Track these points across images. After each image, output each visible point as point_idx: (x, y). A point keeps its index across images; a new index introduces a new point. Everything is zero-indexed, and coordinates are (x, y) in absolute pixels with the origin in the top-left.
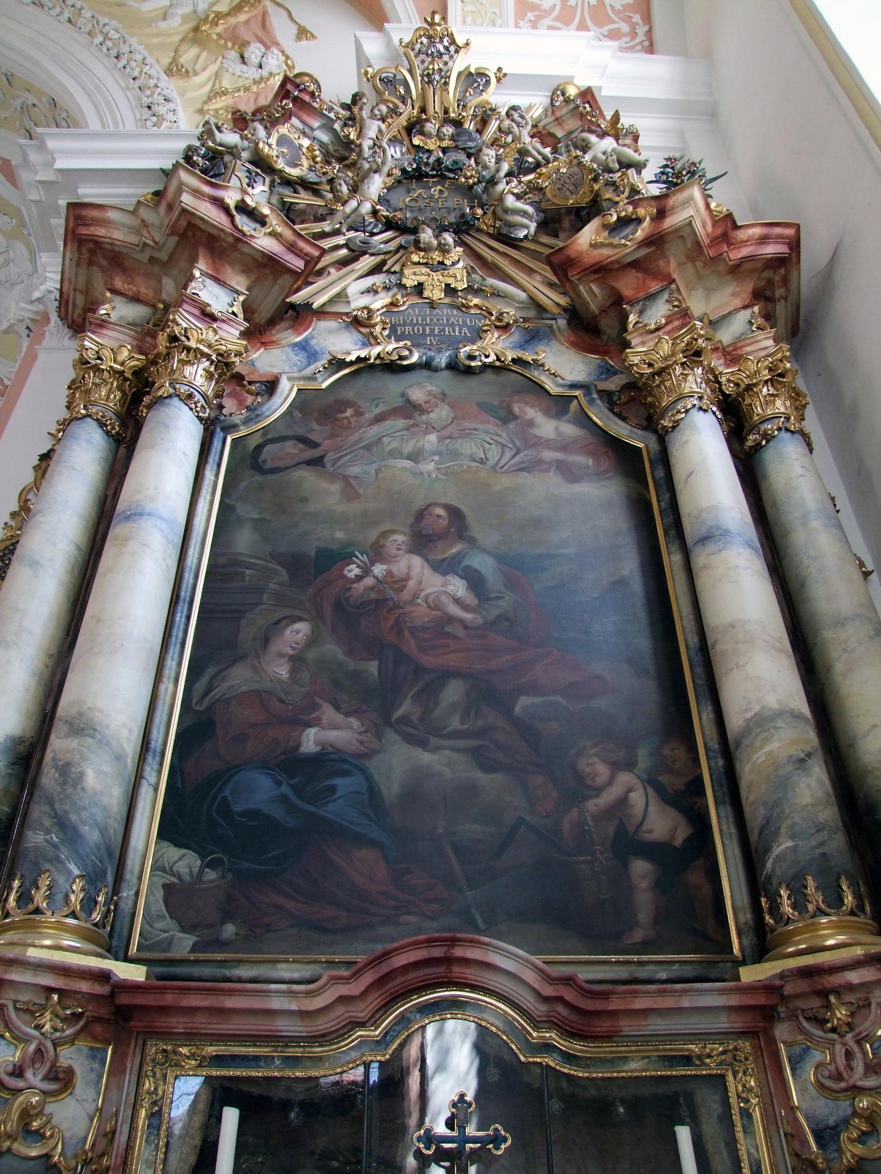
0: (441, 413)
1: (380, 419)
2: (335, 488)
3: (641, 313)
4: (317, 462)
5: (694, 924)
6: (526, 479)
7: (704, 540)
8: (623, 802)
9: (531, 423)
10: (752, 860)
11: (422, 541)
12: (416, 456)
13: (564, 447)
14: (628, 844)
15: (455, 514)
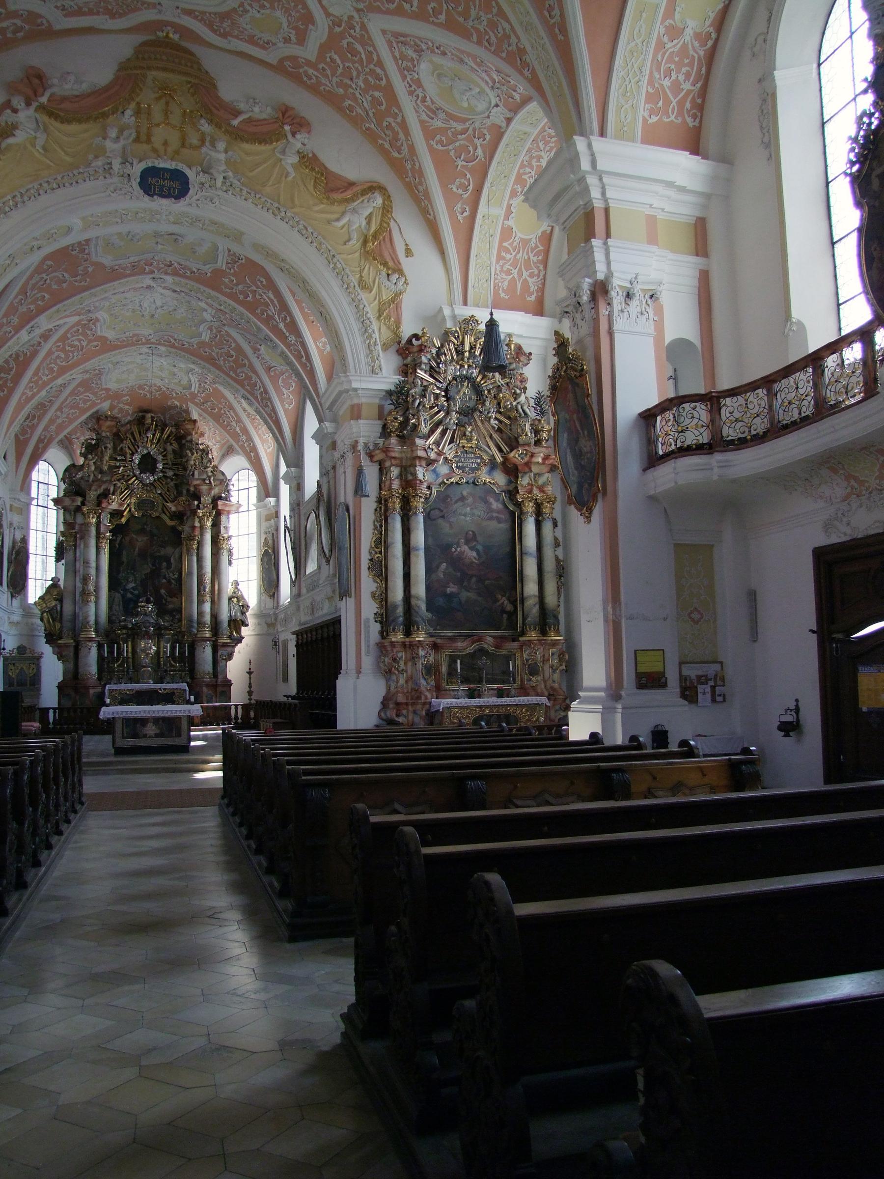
0: (470, 500)
1: (456, 502)
2: (448, 525)
3: (522, 477)
4: (443, 517)
5: (512, 625)
6: (489, 523)
7: (526, 554)
8: (503, 603)
9: (491, 504)
10: (524, 619)
11: (467, 542)
12: (465, 515)
13: (498, 512)
14: (503, 611)
15: (473, 532)
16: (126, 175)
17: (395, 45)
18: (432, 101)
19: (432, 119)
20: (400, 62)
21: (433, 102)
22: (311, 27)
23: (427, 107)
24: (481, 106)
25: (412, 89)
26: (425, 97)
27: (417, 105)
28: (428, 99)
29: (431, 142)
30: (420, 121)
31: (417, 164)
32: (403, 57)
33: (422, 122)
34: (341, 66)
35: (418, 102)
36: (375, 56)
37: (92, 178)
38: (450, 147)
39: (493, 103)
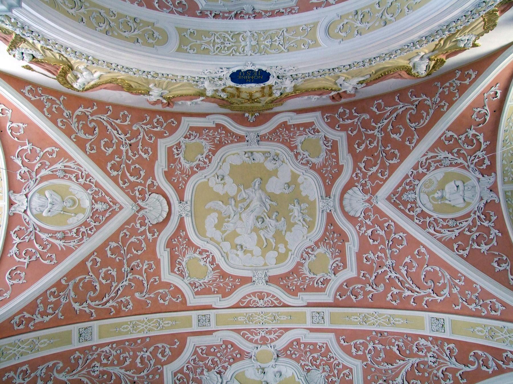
16: (280, 77)
17: (111, 204)
18: (70, 179)
19: (65, 166)
20: (103, 194)
21: (70, 179)
22: (166, 170)
23: (72, 172)
24: (36, 202)
25: (88, 180)
26: (77, 180)
27: (80, 170)
28: (74, 179)
29: (57, 150)
30: (74, 160)
31: (60, 124)
32: (103, 200)
33: (71, 159)
34: (140, 152)
35: (80, 173)
36: (121, 182)
37: (307, 75)
38: (42, 153)
39: (29, 212)
